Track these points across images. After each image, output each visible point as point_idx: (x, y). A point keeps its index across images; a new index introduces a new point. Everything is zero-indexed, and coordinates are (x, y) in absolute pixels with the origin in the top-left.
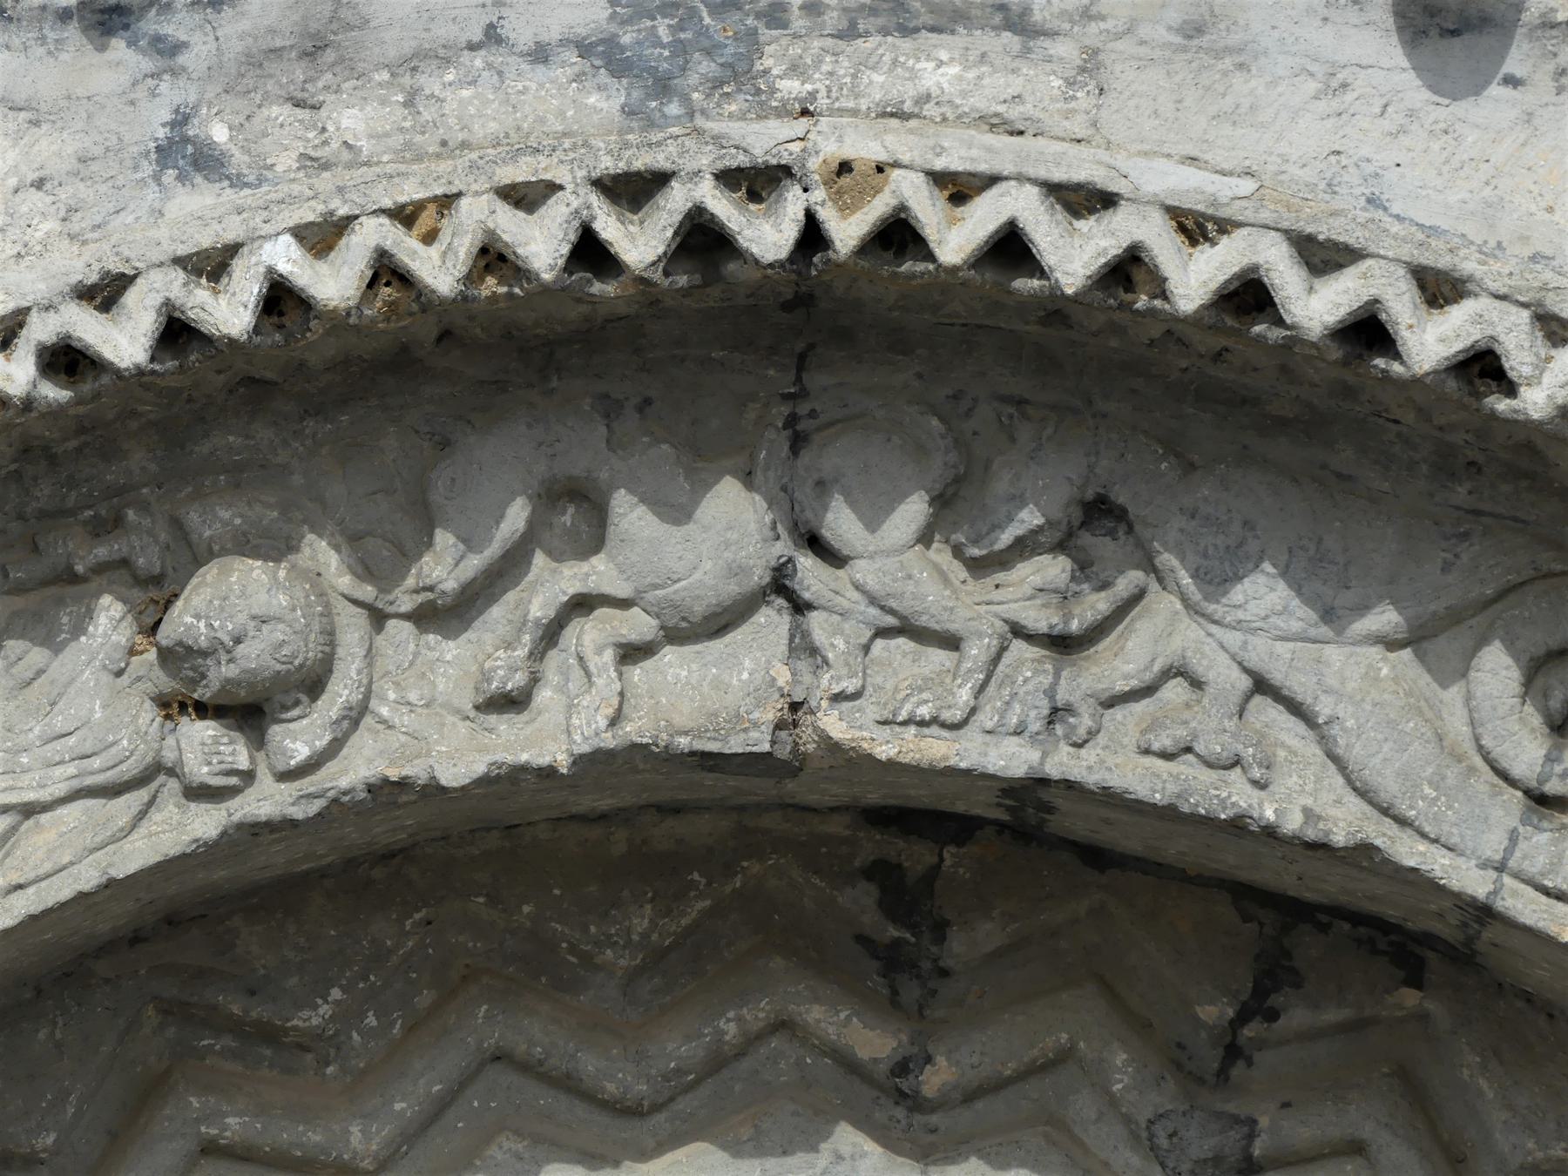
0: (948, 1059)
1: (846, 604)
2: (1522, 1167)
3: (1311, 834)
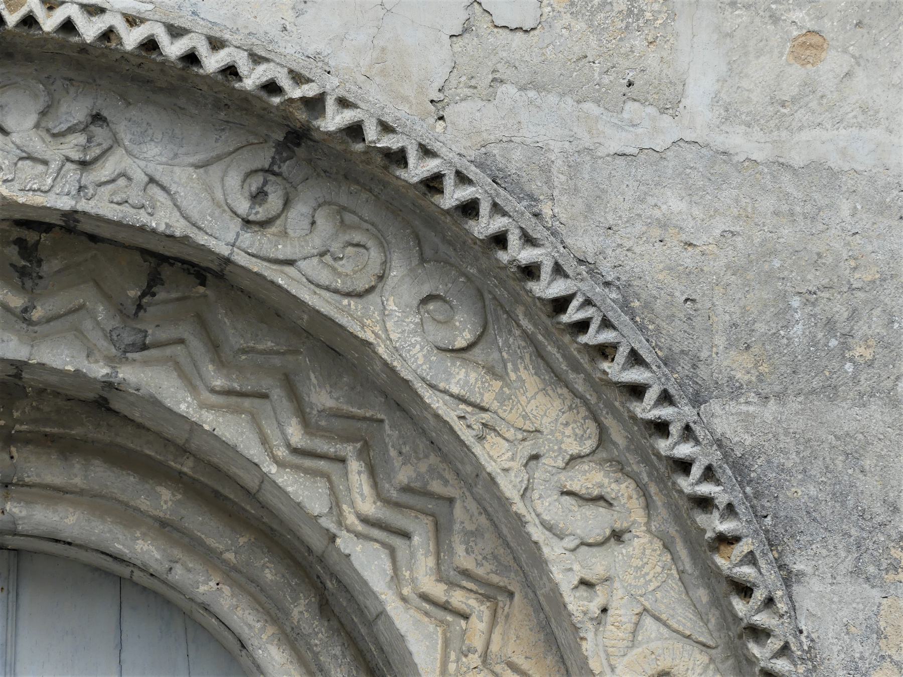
0: (42, 308)
1: (9, 149)
2: (239, 349)
3: (168, 232)
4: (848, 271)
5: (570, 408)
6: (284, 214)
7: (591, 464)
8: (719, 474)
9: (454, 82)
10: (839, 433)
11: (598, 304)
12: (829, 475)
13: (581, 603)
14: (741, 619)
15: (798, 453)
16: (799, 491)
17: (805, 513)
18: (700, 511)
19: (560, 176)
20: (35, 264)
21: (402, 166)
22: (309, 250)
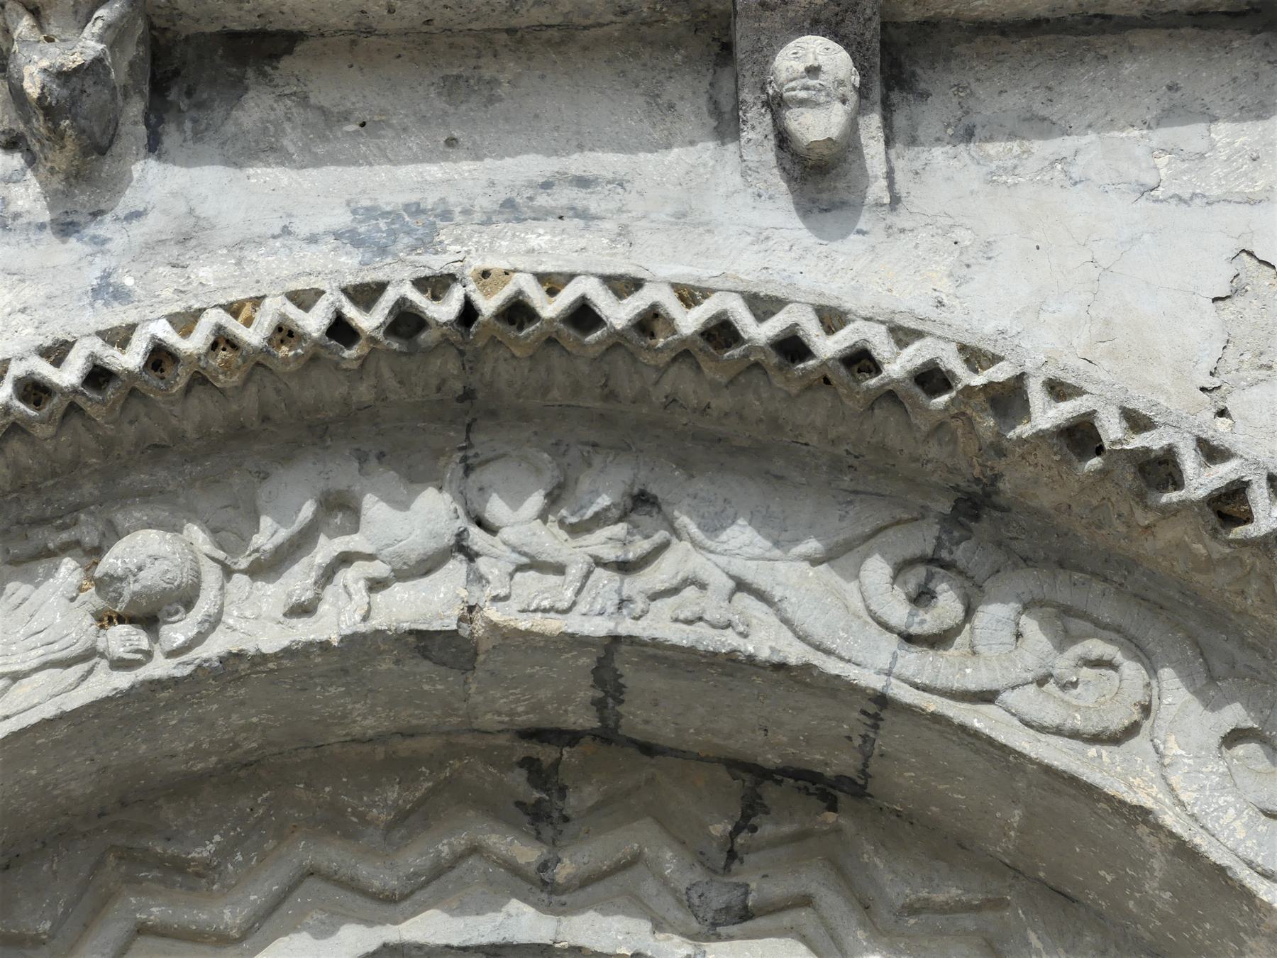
0: (570, 860)
1: (498, 552)
2: (903, 907)
3: (776, 659)
6: (968, 626)
9: (1232, 362)
20: (555, 795)
21: (1170, 487)
22: (1017, 674)
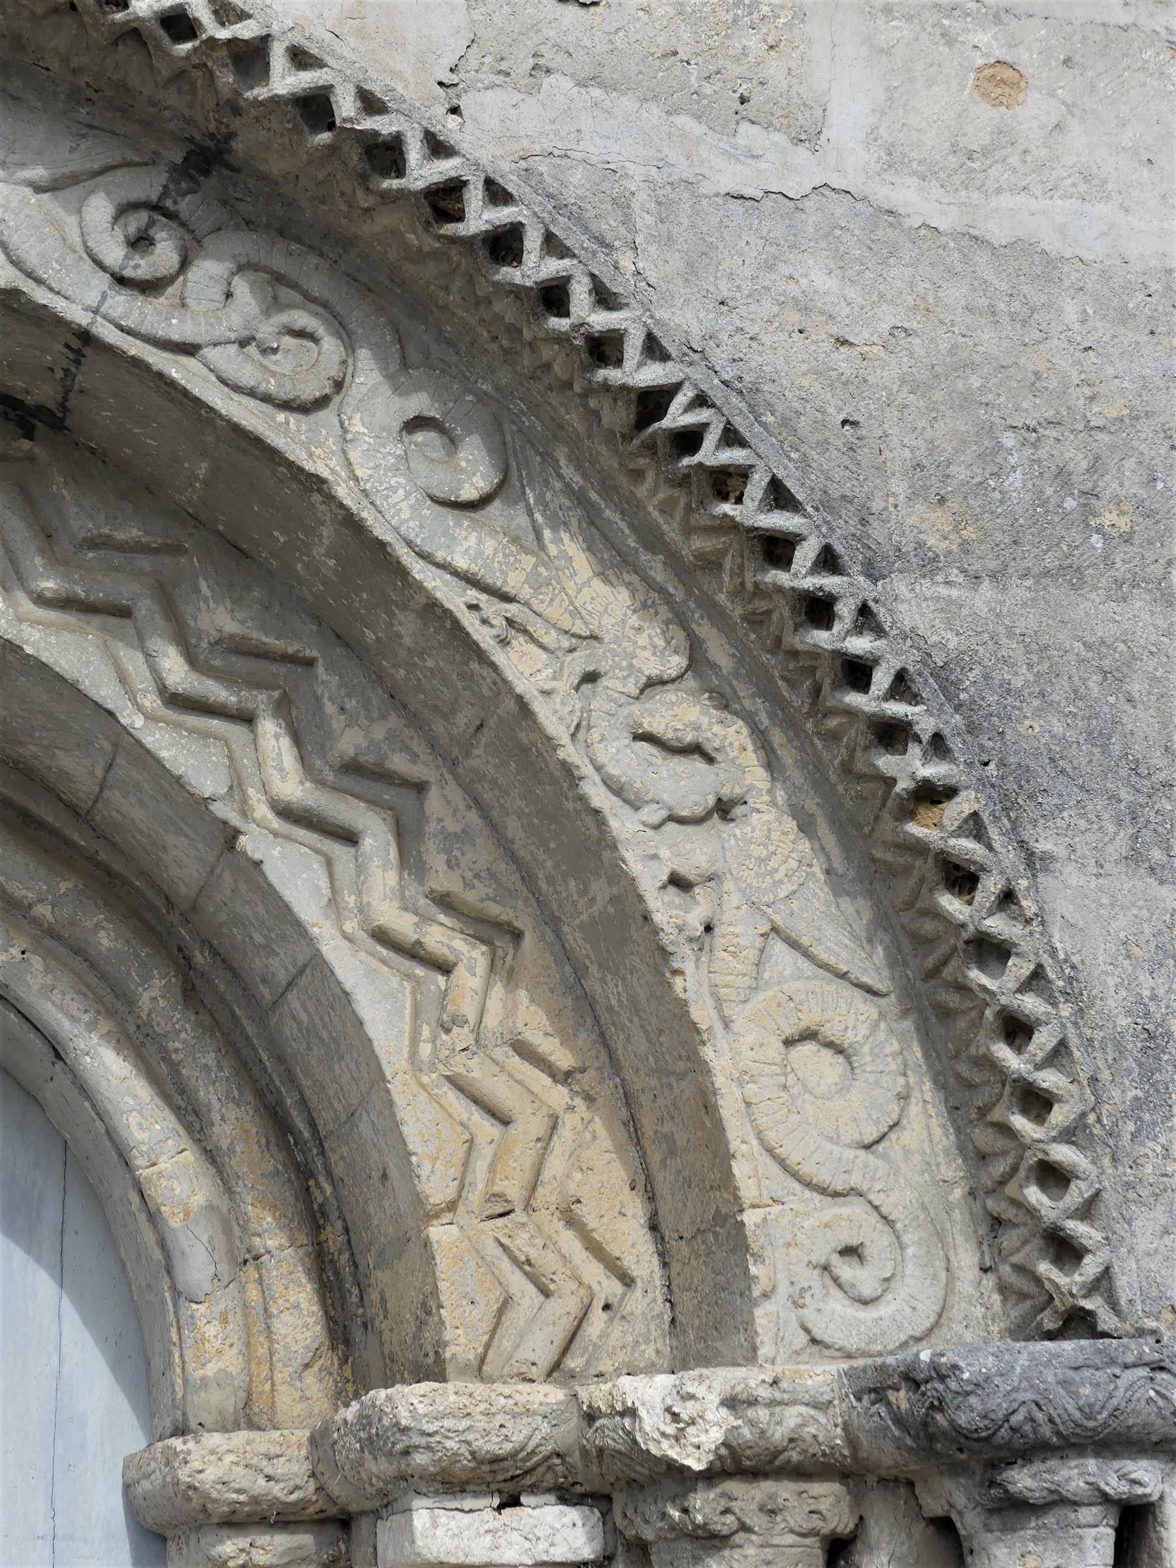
2: (84, 540)
4: (1081, 402)
5: (644, 606)
6: (181, 278)
7: (679, 693)
8: (918, 685)
9: (473, 63)
10: (1091, 639)
11: (718, 403)
12: (1080, 704)
13: (675, 912)
14: (963, 926)
15: (1030, 666)
16: (1036, 726)
17: (1047, 761)
18: (882, 750)
19: (645, 215)
21: (393, 174)
